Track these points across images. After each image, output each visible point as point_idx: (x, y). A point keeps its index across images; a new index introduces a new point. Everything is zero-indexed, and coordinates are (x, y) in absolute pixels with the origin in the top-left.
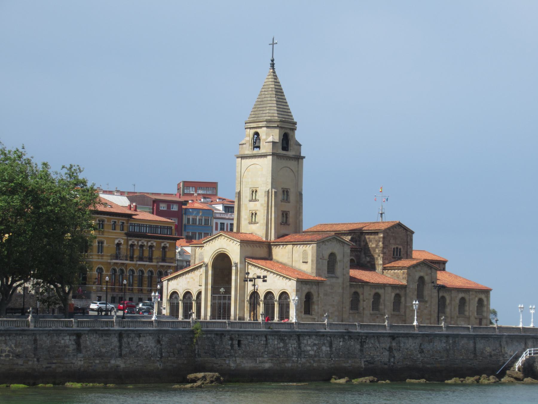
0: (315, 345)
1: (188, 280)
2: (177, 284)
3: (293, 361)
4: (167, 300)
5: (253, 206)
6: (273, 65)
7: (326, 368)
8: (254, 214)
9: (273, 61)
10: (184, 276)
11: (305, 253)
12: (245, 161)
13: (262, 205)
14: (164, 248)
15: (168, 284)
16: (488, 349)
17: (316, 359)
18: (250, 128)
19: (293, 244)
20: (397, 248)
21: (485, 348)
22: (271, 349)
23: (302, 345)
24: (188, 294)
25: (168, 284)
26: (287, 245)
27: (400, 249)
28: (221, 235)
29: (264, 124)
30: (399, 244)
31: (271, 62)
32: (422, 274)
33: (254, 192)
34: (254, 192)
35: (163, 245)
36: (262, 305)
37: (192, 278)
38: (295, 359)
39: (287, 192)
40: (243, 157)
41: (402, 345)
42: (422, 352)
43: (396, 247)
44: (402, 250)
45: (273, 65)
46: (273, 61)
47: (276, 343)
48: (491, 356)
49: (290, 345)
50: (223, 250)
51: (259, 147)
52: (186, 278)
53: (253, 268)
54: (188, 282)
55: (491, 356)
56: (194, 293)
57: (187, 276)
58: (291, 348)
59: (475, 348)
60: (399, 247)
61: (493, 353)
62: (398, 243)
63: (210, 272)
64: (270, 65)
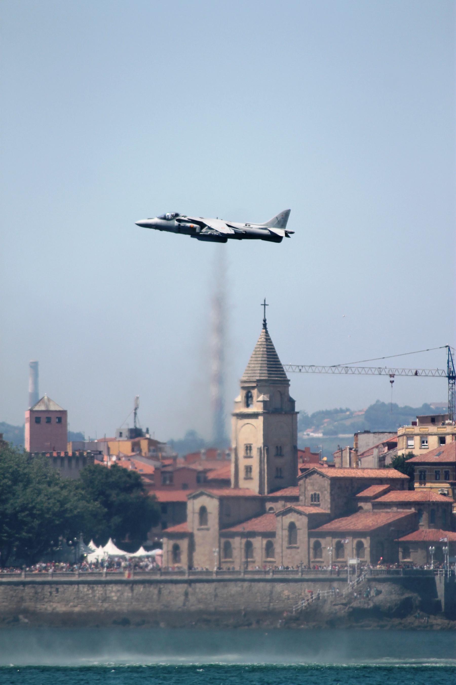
0: (118, 591)
3: (98, 605)
5: (248, 462)
6: (265, 325)
7: (126, 611)
8: (249, 469)
9: (265, 321)
16: (286, 593)
17: (118, 603)
20: (315, 494)
21: (283, 591)
22: (81, 595)
23: (108, 592)
27: (318, 495)
30: (317, 491)
31: (263, 322)
32: (292, 520)
33: (248, 448)
34: (248, 448)
38: (100, 604)
39: (250, 447)
41: (197, 590)
42: (216, 596)
43: (313, 493)
44: (320, 495)
45: (265, 325)
46: (265, 321)
47: (86, 590)
48: (288, 599)
49: (97, 592)
55: (288, 599)
58: (98, 595)
59: (271, 592)
60: (317, 493)
61: (291, 596)
62: (316, 488)
64: (262, 325)
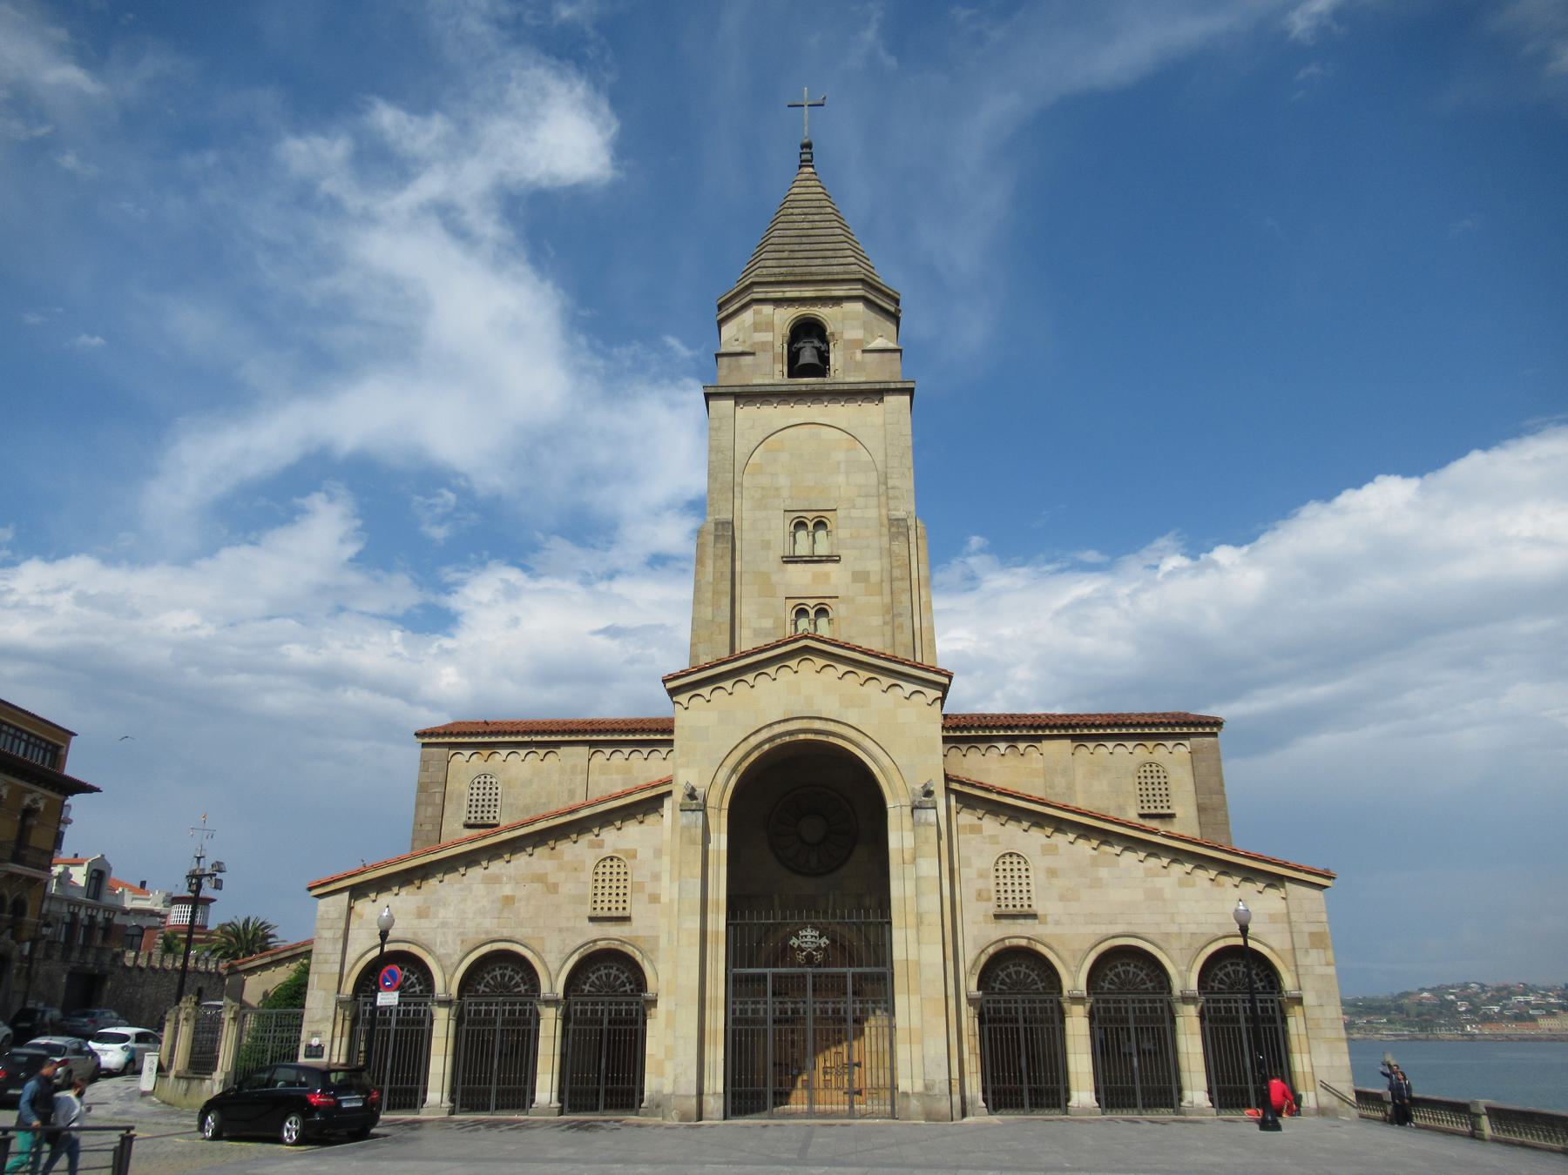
1: (507, 890)
2: (422, 914)
4: (340, 1003)
10: (476, 873)
11: (1152, 778)
12: (747, 413)
13: (860, 577)
14: (29, 812)
15: (350, 908)
18: (778, 302)
19: (1074, 738)
24: (500, 973)
25: (350, 908)
26: (1039, 739)
28: (806, 649)
29: (858, 290)
35: (27, 801)
36: (1077, 1026)
37: (540, 878)
40: (745, 396)
50: (817, 725)
51: (821, 367)
52: (496, 880)
53: (990, 825)
54: (509, 900)
56: (553, 960)
57: (497, 867)
63: (720, 842)
